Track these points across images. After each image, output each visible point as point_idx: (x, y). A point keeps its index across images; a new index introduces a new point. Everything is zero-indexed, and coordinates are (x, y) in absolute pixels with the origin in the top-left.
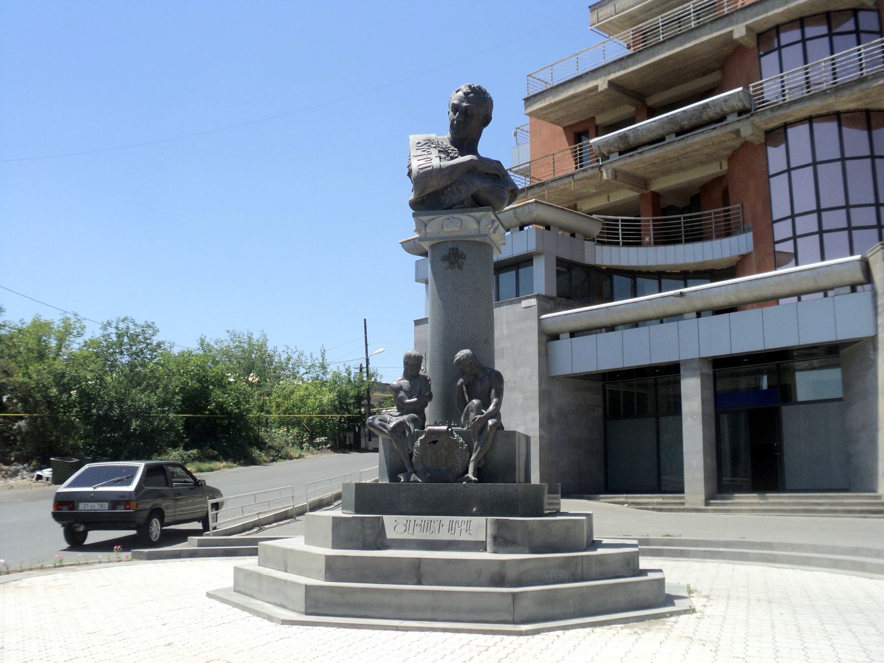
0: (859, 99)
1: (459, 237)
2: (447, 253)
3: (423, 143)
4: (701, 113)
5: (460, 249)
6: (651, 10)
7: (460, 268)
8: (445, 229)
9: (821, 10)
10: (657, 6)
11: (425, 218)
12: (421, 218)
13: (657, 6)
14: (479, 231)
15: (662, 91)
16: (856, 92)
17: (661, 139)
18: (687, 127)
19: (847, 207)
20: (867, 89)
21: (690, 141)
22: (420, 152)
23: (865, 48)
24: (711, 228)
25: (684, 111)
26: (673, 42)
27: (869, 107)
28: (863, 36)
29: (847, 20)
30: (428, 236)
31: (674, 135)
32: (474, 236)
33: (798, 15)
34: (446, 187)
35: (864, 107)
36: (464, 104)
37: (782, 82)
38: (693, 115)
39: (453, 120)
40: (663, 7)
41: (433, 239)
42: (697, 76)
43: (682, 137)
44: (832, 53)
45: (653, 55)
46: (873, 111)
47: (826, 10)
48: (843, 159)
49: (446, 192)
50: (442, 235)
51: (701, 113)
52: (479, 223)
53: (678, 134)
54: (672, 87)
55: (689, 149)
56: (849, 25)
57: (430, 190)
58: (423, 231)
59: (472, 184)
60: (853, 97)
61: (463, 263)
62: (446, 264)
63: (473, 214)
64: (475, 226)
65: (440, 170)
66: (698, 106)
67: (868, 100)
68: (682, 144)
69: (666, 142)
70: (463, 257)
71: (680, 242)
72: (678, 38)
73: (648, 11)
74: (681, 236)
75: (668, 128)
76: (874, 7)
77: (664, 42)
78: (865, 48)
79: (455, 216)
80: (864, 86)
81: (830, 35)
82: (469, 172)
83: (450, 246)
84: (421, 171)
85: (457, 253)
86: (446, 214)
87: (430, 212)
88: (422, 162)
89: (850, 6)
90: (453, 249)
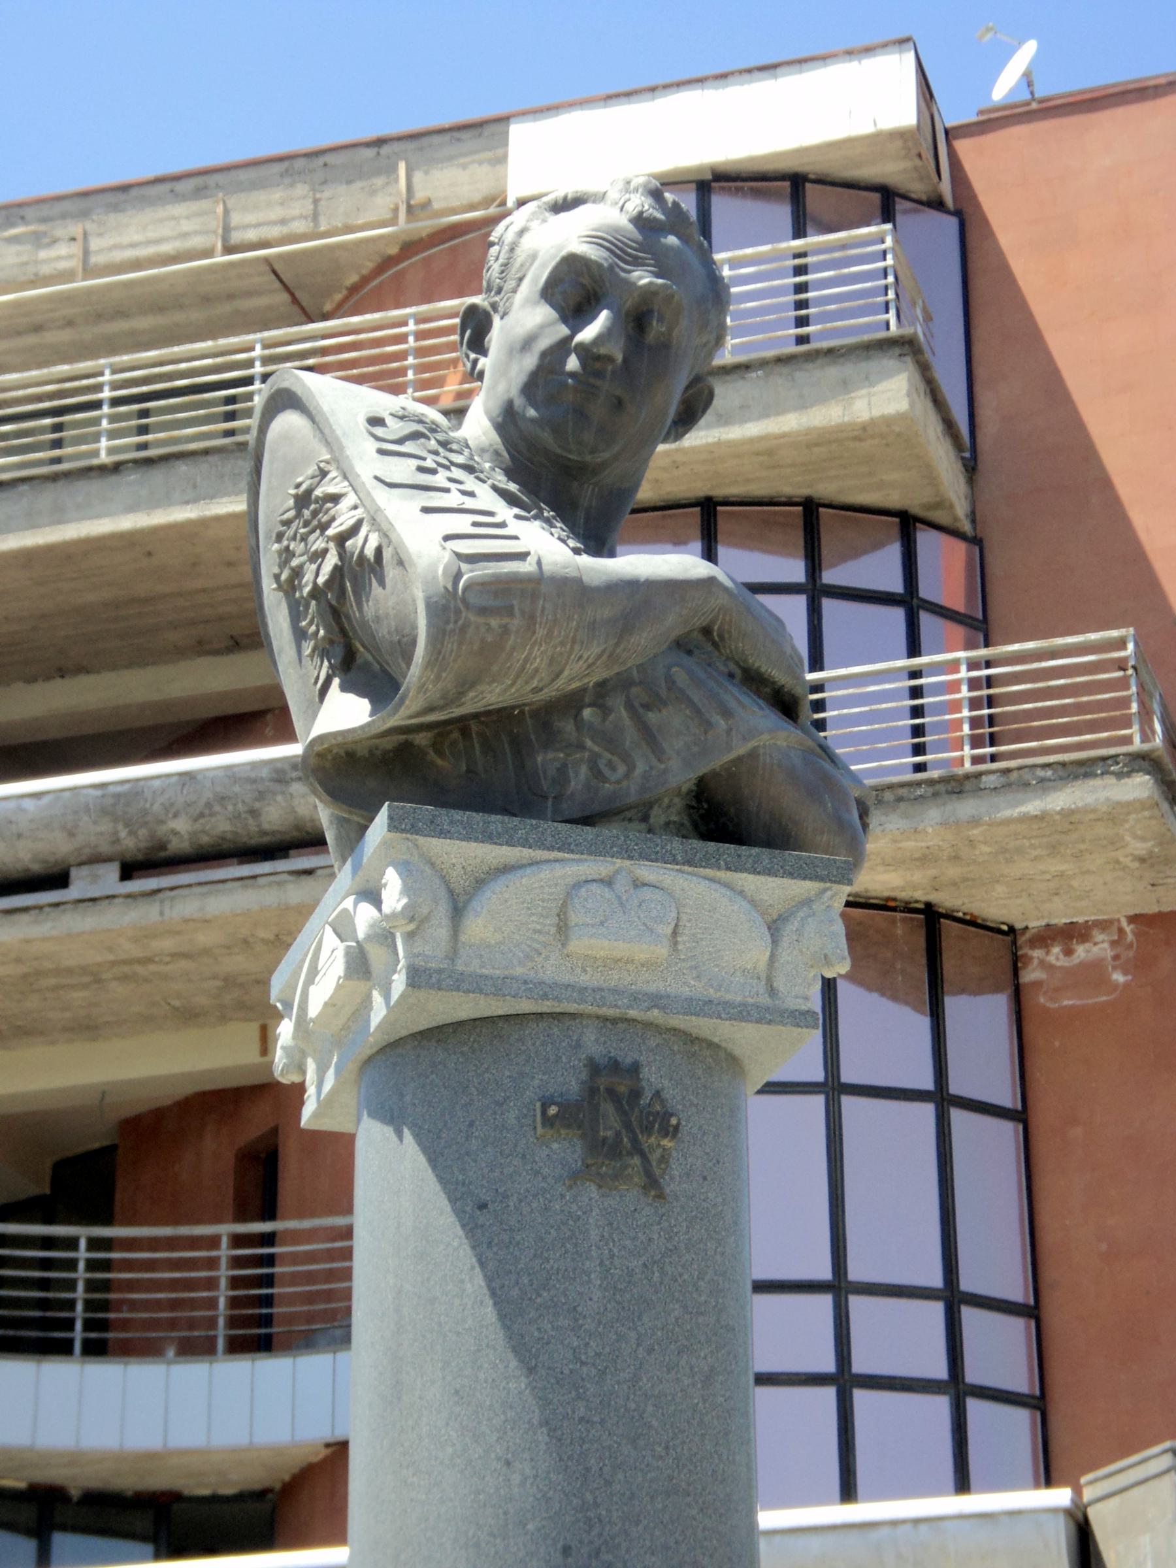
0: (924, 859)
1: (657, 1000)
2: (571, 1084)
3: (396, 428)
4: (261, 796)
5: (653, 1076)
6: (38, 328)
7: (652, 1184)
8: (579, 944)
9: (788, 490)
10: (70, 323)
11: (461, 852)
12: (436, 846)
13: (70, 323)
14: (772, 991)
15: (31, 680)
16: (931, 825)
17: (57, 879)
18: (178, 846)
19: (839, 1286)
20: (975, 822)
21: (186, 907)
22: (403, 470)
23: (973, 665)
24: (212, 1303)
25: (188, 777)
26: (157, 476)
27: (945, 900)
28: (926, 620)
29: (877, 546)
30: (468, 964)
31: (112, 872)
32: (742, 1013)
33: (700, 489)
34: (571, 703)
35: (921, 896)
36: (643, 278)
37: (916, 692)
38: (222, 799)
39: (562, 347)
40: (88, 333)
41: (498, 987)
42: (202, 648)
43: (151, 883)
44: (914, 650)
45: (59, 516)
46: (950, 916)
47: (805, 492)
48: (833, 1088)
49: (568, 727)
50: (552, 969)
51: (261, 796)
52: (775, 928)
53: (129, 871)
54: (82, 669)
55: (167, 944)
56: (881, 568)
57: (492, 695)
58: (440, 931)
59: (727, 713)
60: (909, 845)
61: (664, 1159)
62: (566, 1150)
63: (748, 881)
64: (757, 954)
65: (572, 590)
66: (254, 765)
67: (953, 872)
68: (149, 914)
69: (74, 891)
70: (664, 1123)
71: (63, 1349)
72: (182, 468)
73: (19, 333)
74: (69, 1324)
75: (96, 833)
76: (967, 527)
77: (116, 468)
78: (973, 665)
79: (647, 871)
80: (966, 808)
81: (815, 592)
82: (682, 645)
83: (594, 1044)
84: (469, 573)
85: (636, 1094)
86: (596, 850)
87: (497, 821)
88: (462, 524)
89: (894, 499)
90: (615, 1066)
